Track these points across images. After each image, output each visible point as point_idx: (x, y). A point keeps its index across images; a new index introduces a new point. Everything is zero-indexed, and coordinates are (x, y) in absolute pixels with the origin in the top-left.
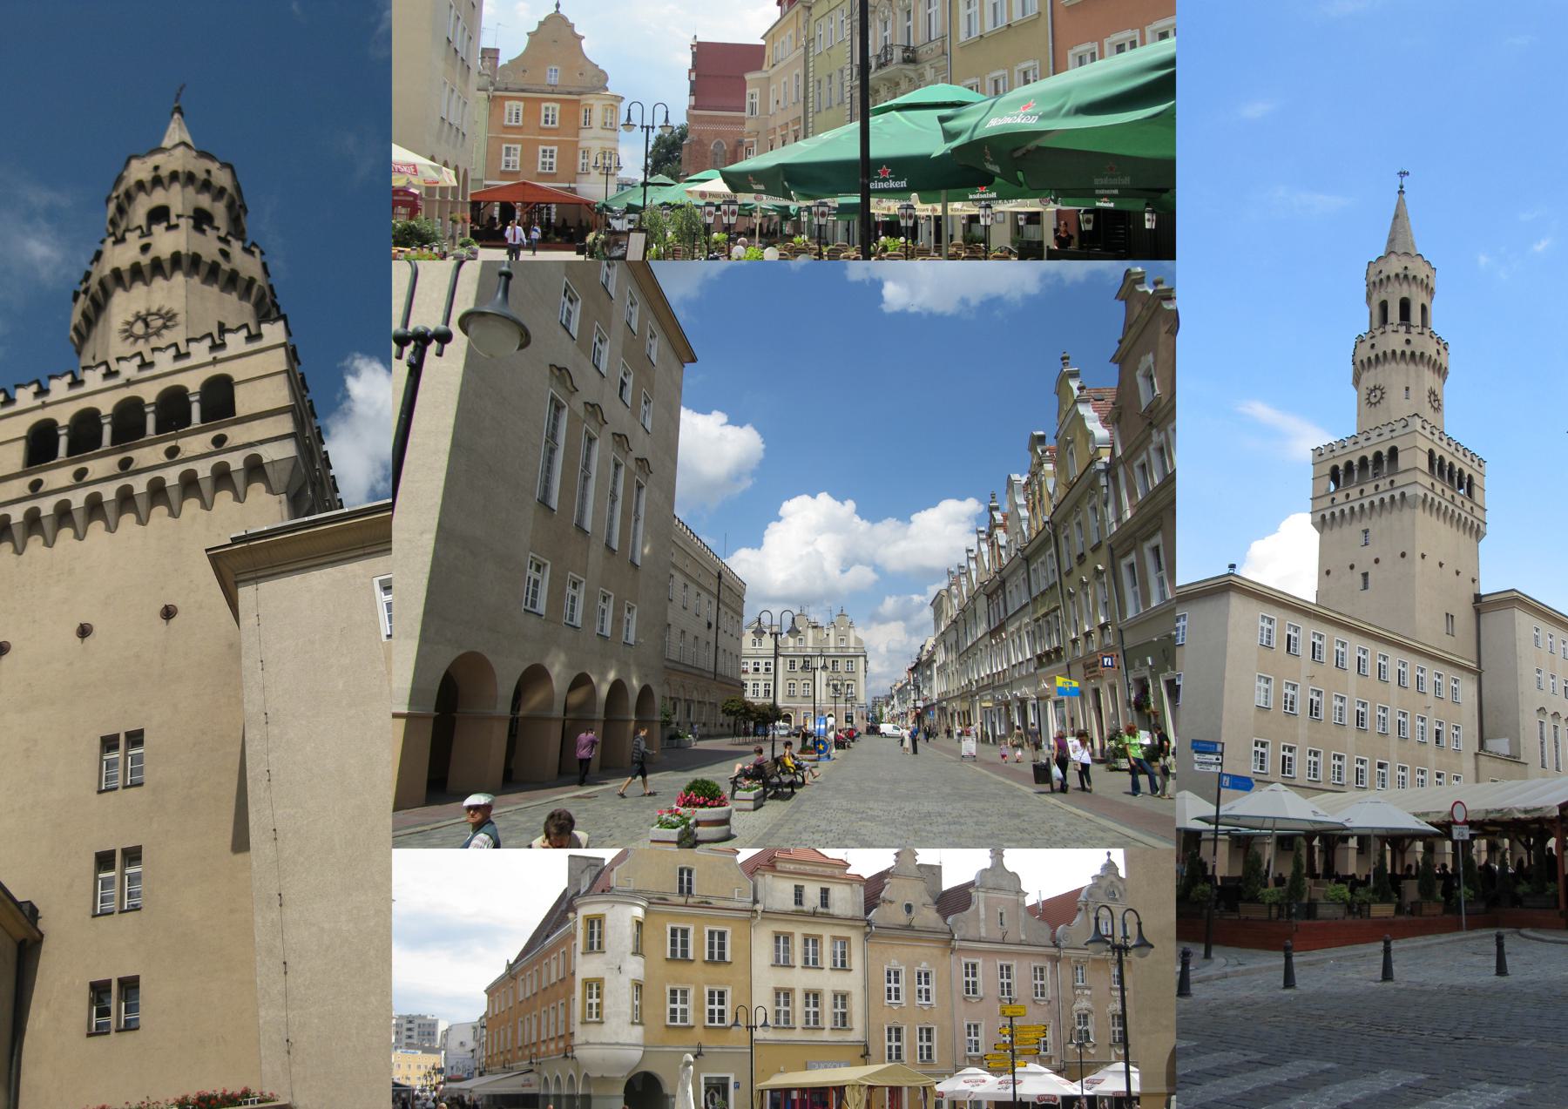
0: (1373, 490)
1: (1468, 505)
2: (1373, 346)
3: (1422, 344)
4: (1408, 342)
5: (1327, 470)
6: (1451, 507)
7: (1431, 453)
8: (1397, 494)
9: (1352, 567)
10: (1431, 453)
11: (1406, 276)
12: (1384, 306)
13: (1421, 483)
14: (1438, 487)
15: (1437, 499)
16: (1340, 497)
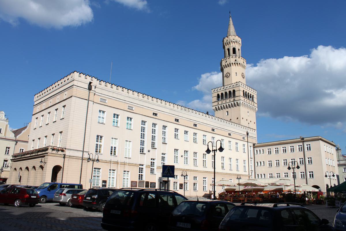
0: (229, 101)
1: (253, 103)
4: (236, 60)
7: (244, 91)
8: (235, 102)
10: (244, 91)
13: (242, 100)
14: (246, 100)
15: (245, 103)
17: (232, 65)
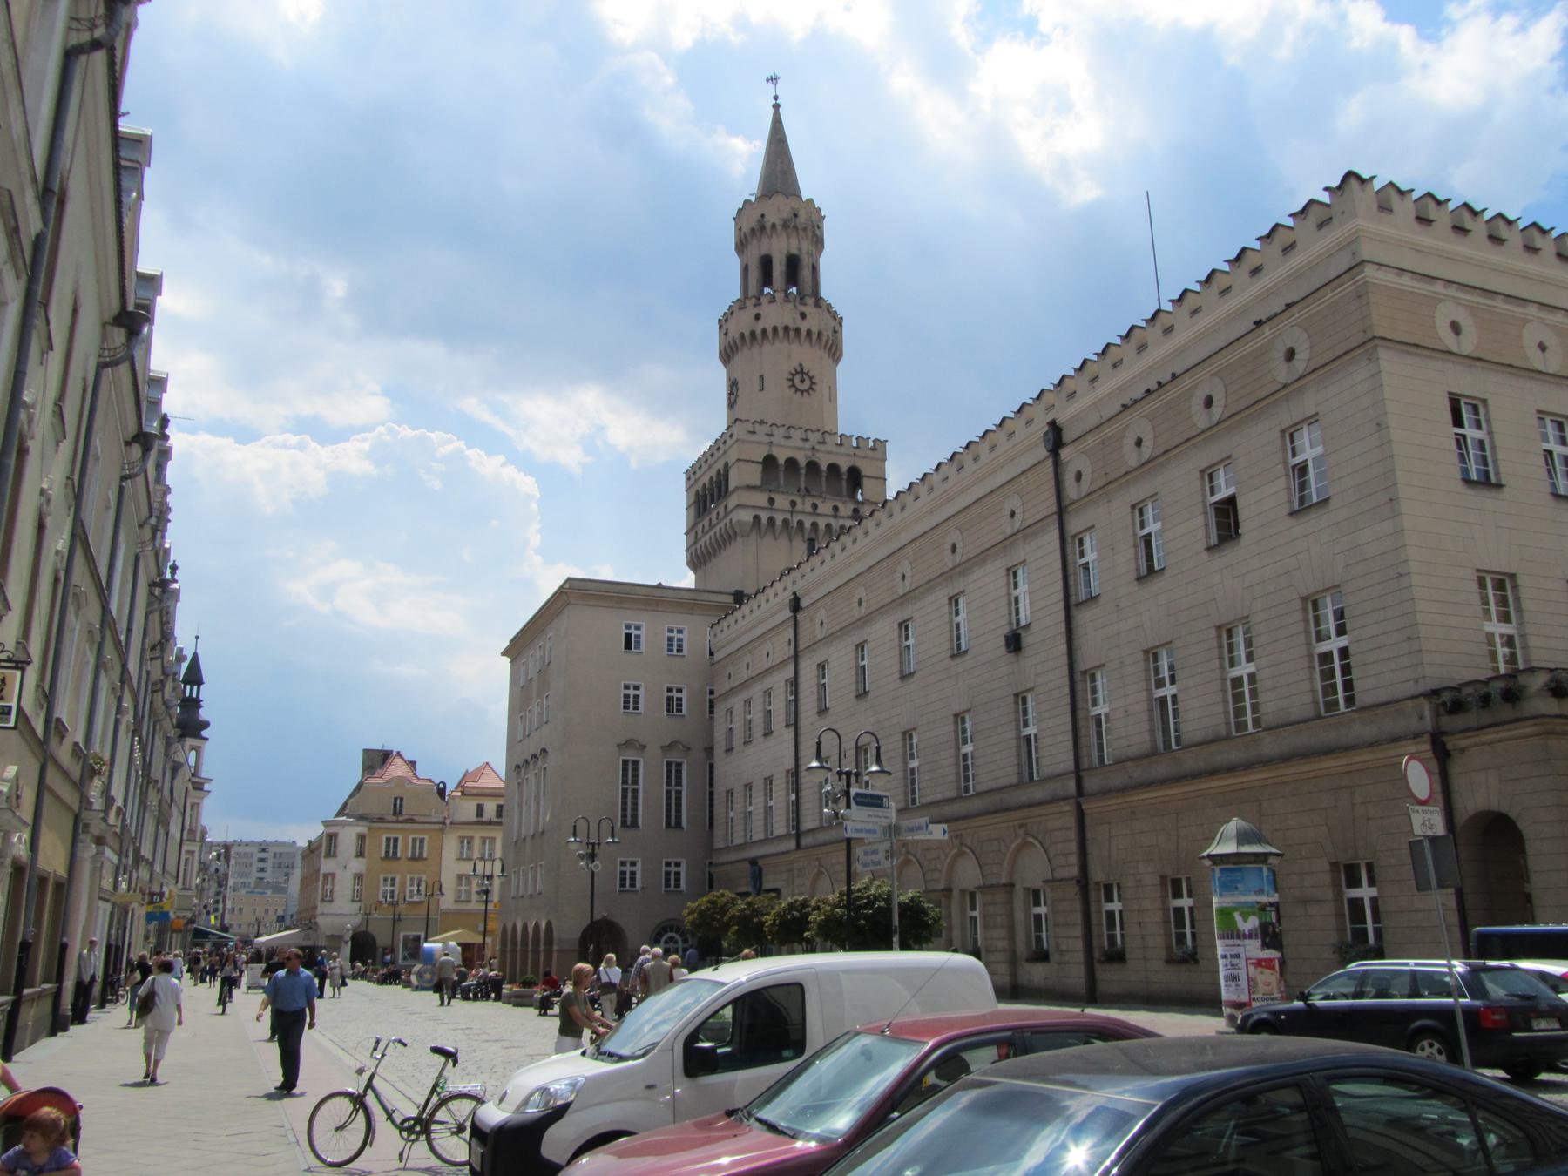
2: (758, 317)
4: (803, 316)
11: (795, 227)
12: (766, 263)
17: (781, 333)
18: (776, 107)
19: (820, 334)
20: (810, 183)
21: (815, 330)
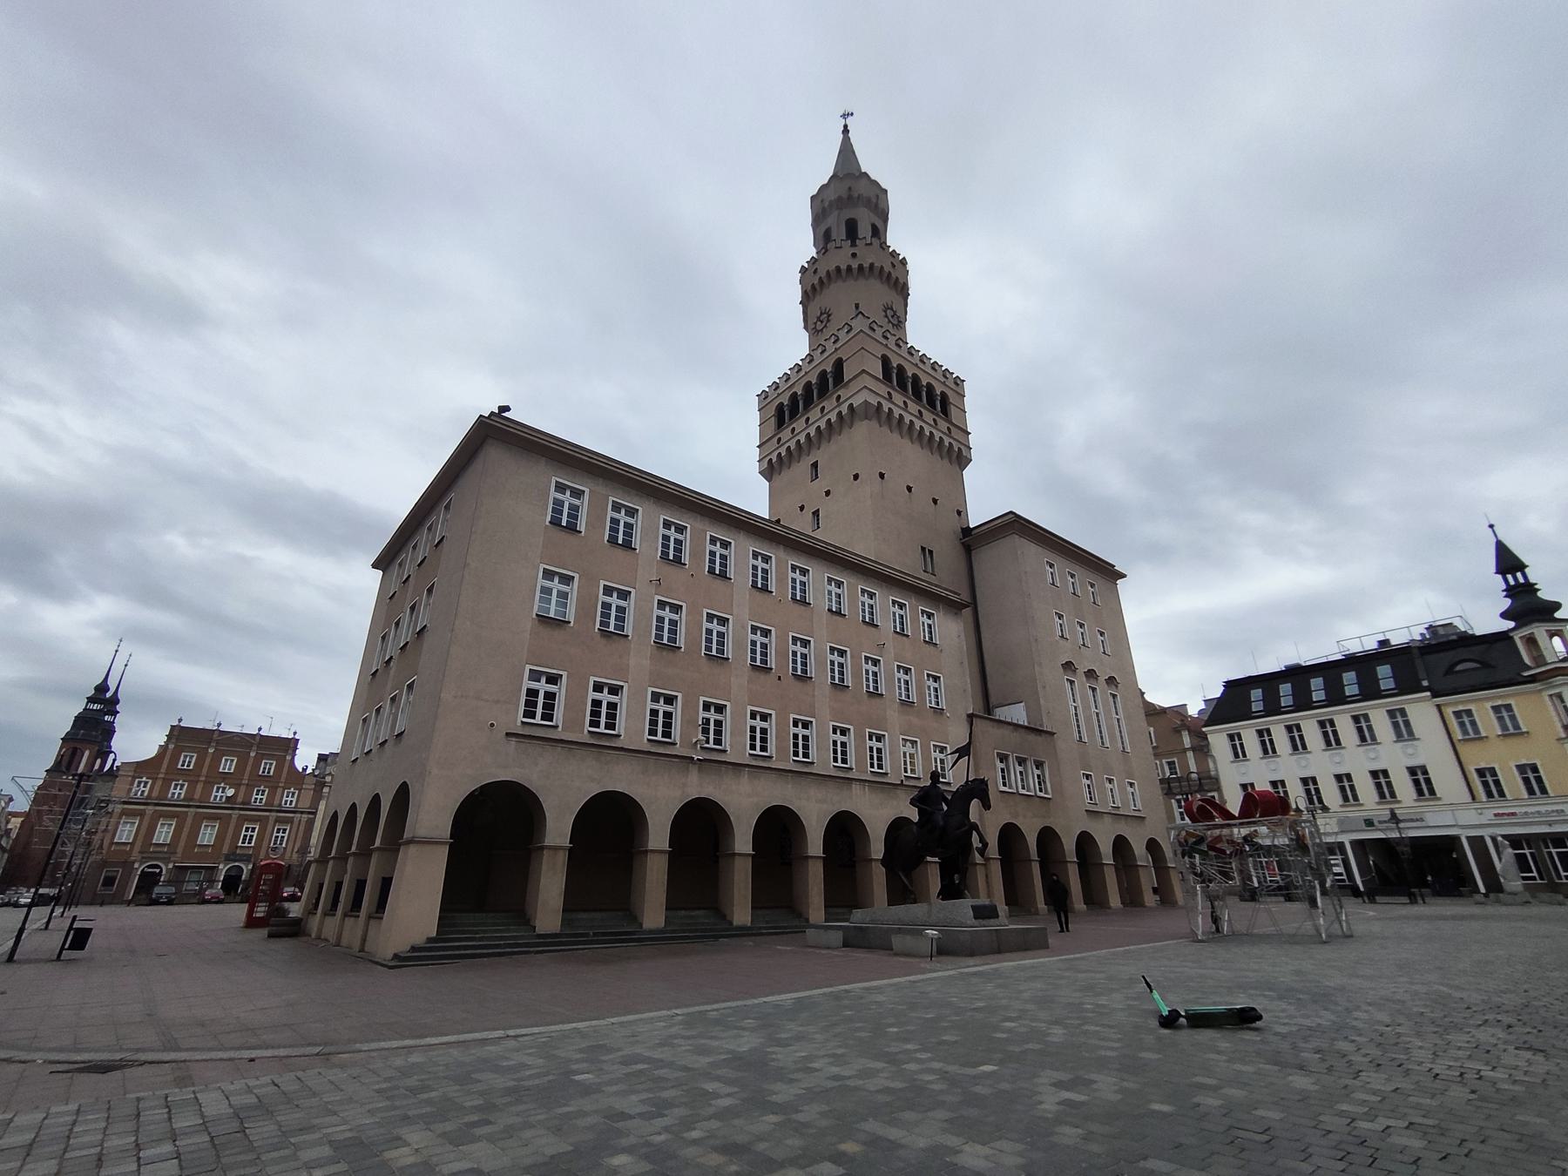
0: (817, 418)
1: (943, 425)
3: (867, 257)
4: (854, 255)
5: (772, 410)
6: (918, 423)
7: (885, 361)
9: (802, 508)
10: (885, 361)
11: (850, 197)
14: (898, 398)
16: (786, 434)
18: (846, 130)
19: (872, 265)
20: (869, 163)
21: (866, 265)
